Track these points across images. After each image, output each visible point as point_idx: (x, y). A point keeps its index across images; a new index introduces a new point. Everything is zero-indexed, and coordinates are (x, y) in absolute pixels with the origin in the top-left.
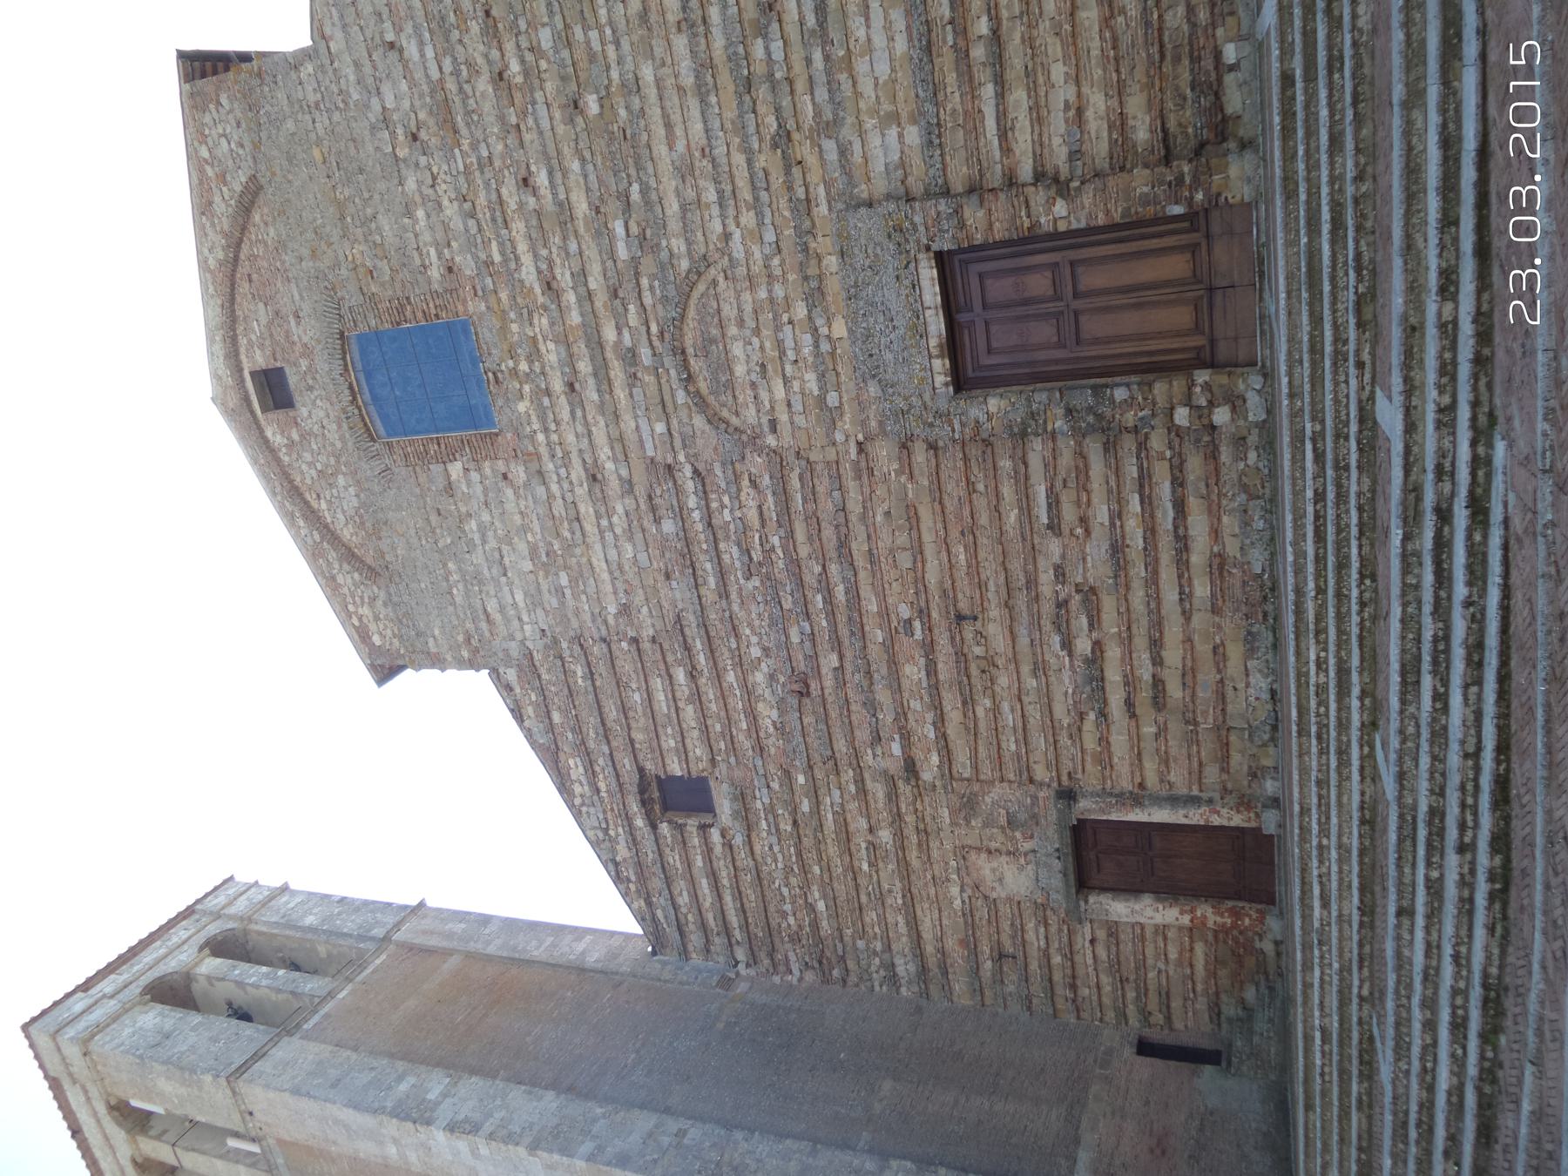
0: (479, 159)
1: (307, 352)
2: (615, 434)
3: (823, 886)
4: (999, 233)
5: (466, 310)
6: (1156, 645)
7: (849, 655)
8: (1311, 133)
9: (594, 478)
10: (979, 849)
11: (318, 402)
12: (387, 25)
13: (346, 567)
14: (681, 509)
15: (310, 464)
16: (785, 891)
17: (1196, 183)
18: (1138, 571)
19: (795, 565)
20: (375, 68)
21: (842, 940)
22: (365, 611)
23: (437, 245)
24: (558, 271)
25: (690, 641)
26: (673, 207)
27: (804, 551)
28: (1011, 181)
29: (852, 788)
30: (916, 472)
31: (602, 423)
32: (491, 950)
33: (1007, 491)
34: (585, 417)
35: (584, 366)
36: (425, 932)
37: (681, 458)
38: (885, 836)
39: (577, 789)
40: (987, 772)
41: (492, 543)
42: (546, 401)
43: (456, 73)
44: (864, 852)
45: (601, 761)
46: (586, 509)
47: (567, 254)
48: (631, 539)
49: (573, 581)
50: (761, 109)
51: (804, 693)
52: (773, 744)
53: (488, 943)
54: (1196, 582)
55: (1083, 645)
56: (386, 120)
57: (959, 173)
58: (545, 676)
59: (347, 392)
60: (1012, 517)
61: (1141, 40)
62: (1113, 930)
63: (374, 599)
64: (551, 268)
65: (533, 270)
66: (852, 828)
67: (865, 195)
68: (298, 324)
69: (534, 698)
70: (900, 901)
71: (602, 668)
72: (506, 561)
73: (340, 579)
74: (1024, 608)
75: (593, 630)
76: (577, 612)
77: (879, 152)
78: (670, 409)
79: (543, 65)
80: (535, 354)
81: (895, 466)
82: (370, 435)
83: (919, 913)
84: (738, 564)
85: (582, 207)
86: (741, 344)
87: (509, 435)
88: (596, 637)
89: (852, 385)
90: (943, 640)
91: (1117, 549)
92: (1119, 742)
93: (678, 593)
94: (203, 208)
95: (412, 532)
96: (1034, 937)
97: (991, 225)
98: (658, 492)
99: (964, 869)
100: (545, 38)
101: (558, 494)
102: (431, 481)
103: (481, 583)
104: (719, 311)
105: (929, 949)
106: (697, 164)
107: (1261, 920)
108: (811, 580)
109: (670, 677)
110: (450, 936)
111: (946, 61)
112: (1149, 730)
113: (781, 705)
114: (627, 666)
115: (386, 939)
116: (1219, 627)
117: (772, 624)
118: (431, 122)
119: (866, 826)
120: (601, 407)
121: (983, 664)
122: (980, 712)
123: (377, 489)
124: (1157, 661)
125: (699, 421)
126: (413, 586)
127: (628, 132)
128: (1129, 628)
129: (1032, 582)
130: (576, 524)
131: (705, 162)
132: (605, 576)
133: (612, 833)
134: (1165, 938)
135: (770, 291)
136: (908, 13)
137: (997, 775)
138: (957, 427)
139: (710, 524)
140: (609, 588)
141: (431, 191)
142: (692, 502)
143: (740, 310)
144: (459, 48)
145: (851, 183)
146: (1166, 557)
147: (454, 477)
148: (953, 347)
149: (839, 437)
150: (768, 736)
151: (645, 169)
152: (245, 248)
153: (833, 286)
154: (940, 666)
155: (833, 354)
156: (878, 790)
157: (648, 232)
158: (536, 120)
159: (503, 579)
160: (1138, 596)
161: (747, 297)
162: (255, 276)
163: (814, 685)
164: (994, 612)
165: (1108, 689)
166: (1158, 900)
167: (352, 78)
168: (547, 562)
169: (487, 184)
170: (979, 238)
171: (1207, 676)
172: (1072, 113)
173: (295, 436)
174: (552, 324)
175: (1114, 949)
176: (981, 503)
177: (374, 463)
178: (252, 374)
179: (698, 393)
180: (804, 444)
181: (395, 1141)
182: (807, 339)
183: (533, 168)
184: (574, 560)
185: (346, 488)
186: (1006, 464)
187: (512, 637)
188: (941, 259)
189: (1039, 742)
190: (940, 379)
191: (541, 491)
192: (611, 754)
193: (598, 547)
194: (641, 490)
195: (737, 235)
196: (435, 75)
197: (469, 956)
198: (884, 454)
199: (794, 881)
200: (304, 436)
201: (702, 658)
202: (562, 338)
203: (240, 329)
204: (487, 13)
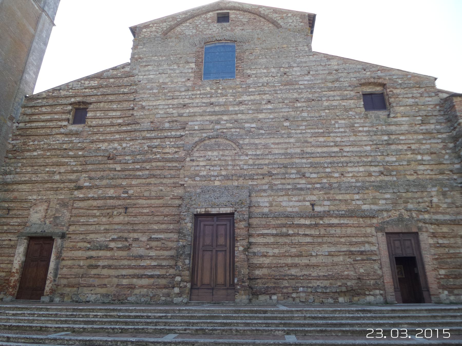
0: (277, 90)
1: (232, 30)
2: (197, 114)
3: (43, 155)
4: (237, 231)
5: (238, 78)
6: (109, 267)
7: (119, 173)
8: (251, 318)
9: (184, 106)
10: (48, 206)
11: (218, 30)
12: (314, 73)
13: (168, 26)
14: (172, 130)
16: (42, 143)
17: (242, 286)
18: (133, 263)
19: (150, 161)
20: (304, 67)
21: (22, 159)
22: (154, 29)
23: (256, 74)
24: (244, 106)
25: (131, 126)
26: (257, 141)
27: (154, 164)
28: (250, 236)
29: (75, 169)
30: (173, 200)
31: (200, 111)
32: (34, 44)
33: (164, 226)
34: (203, 106)
35: (217, 109)
36: (44, 24)
37: (187, 132)
38: (57, 177)
39: (87, 82)
40: (74, 211)
41: (169, 72)
42: (209, 96)
43: (300, 89)
44: (52, 170)
45: (95, 91)
47: (249, 110)
48: (165, 113)
49: (154, 94)
50: (279, 170)
51: (109, 158)
52: (94, 146)
53: (37, 43)
54: (127, 280)
55: (112, 245)
56: (291, 67)
57: (254, 221)
58: (125, 79)
59: (220, 39)
60: (155, 227)
61: (281, 273)
62: (14, 247)
63: (157, 32)
64: (245, 104)
65: (246, 99)
66: (61, 167)
67: (252, 195)
68: (241, 29)
69: (119, 74)
70: (33, 179)
71: (126, 97)
72: (163, 75)
73: (165, 24)
74: (127, 228)
75: (138, 97)
76: (144, 93)
77: (263, 200)
78: (202, 131)
79: (298, 113)
80: (222, 95)
82: (206, 43)
83: (28, 185)
84: (153, 144)
85: (261, 116)
86: (217, 155)
87: (200, 83)
88: (136, 97)
89: (201, 185)
91: (141, 257)
92: (79, 254)
93: (146, 124)
94: (275, 11)
95: (176, 49)
96: (14, 221)
97: (239, 229)
98: (178, 124)
99: (42, 201)
100: (305, 114)
101: (181, 94)
102: (190, 57)
103: (158, 66)
104: (227, 150)
105: (15, 187)
106: (267, 150)
107: (10, 295)
108: (145, 165)
109: (120, 118)
110: (41, 31)
111: (284, 221)
112: (82, 263)
114: (125, 105)
115: (43, 11)
116: (112, 286)
117: (133, 152)
118: (288, 79)
119: (61, 171)
120: (205, 112)
121: (111, 214)
124: (104, 267)
125: (197, 139)
126: (160, 45)
128: (116, 259)
129: (134, 231)
130: (171, 98)
131: (267, 152)
132: (154, 104)
133: (70, 91)
134: (8, 263)
135: (230, 165)
136: (297, 212)
137: (73, 215)
138: (184, 214)
139: (166, 137)
140: (151, 104)
141: (270, 75)
142: (173, 133)
143: (226, 156)
144: (306, 91)
145: (256, 191)
147: (191, 64)
148: (208, 215)
149: (186, 179)
150: (96, 145)
151: (268, 135)
152: (263, 20)
153: (229, 183)
154: (112, 201)
155: (210, 180)
156: (73, 177)
157: (251, 133)
158: (285, 108)
159: (158, 73)
160: (126, 262)
161: (230, 158)
162: (255, 20)
164: (126, 219)
165: (97, 251)
166: (23, 262)
167: (303, 60)
168: (161, 87)
169: (270, 91)
170: (236, 225)
171: (97, 282)
172: (265, 254)
173: (209, 21)
174: (230, 102)
175: (7, 246)
176: (161, 218)
177: (198, 42)
178: (228, 13)
179: (205, 140)
180: (186, 168)
182: (216, 174)
183: (272, 105)
184: (161, 95)
185: (192, 32)
186: (171, 227)
187: (139, 72)
188: (232, 214)
189: (82, 229)
190: (199, 210)
191: (183, 89)
192: (97, 95)
193: (164, 103)
194: (179, 119)
195: (247, 158)
196: (300, 83)
197: (33, 36)
198: (180, 191)
199: (46, 146)
201: (124, 128)
202: (226, 104)
203: (241, 12)
204: (313, 100)
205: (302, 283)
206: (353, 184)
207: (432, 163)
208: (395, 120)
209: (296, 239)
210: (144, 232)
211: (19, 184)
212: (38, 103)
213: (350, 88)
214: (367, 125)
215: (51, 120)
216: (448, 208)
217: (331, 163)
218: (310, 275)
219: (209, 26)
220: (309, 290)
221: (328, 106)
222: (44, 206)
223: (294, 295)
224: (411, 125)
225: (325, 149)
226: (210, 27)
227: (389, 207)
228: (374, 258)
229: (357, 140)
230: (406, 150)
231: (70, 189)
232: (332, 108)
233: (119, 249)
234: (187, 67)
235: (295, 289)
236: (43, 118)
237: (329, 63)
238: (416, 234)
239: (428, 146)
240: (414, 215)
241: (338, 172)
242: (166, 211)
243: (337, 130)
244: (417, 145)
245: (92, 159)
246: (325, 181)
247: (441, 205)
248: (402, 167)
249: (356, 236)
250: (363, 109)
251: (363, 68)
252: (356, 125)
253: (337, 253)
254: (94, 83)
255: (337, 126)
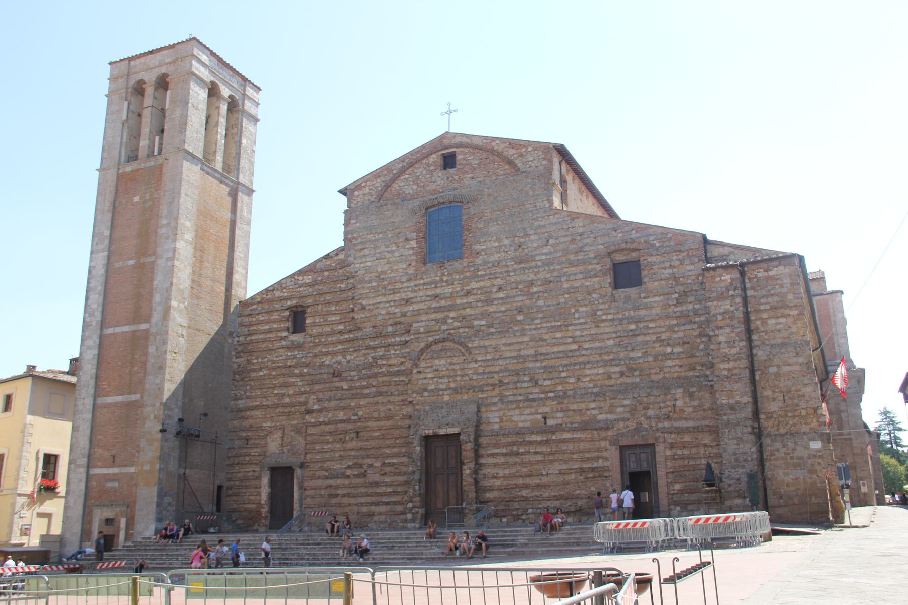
1: (460, 180)
4: (464, 453)
7: (347, 392)
10: (283, 434)
13: (384, 184)
15: (421, 172)
16: (266, 360)
18: (371, 490)
19: (376, 375)
22: (367, 190)
23: (486, 249)
24: (473, 297)
27: (380, 379)
29: (302, 390)
33: (396, 450)
35: (443, 303)
38: (287, 400)
39: (300, 278)
40: (309, 438)
42: (433, 286)
43: (536, 267)
44: (281, 392)
45: (311, 290)
46: (397, 297)
47: (477, 302)
49: (373, 288)
52: (317, 361)
55: (348, 472)
56: (528, 235)
58: (341, 271)
62: (259, 478)
63: (371, 194)
64: (474, 294)
66: (290, 388)
71: (344, 296)
72: (381, 260)
73: (379, 180)
76: (363, 288)
78: (428, 334)
79: (534, 301)
81: (405, 413)
85: (491, 309)
88: (355, 295)
90: (350, 426)
91: (377, 484)
92: (320, 482)
93: (368, 330)
94: (513, 144)
95: (393, 220)
96: (254, 451)
100: (541, 303)
103: (374, 248)
105: (248, 413)
107: (264, 525)
108: (371, 381)
110: (242, 211)
112: (323, 492)
113: (330, 366)
114: (344, 306)
117: (357, 365)
121: (343, 440)
122: (328, 437)
123: (409, 207)
124: (344, 495)
125: (422, 345)
127: (510, 330)
129: (368, 457)
130: (392, 292)
132: (375, 301)
136: (528, 427)
139: (390, 345)
140: (371, 302)
142: (398, 339)
144: (543, 269)
146: (374, 499)
147: (411, 242)
148: (436, 436)
149: (414, 395)
150: (320, 359)
152: (497, 159)
153: (459, 397)
155: (439, 395)
156: (302, 399)
157: (481, 333)
160: (363, 490)
162: (488, 161)
163: (337, 379)
164: (359, 444)
166: (269, 494)
168: (379, 278)
169: (501, 273)
170: (463, 447)
173: (432, 168)
174: (457, 292)
176: (393, 441)
177: (418, 208)
179: (431, 346)
181: (169, 224)
182: (444, 387)
186: (403, 450)
187: (355, 259)
188: (459, 434)
189: (318, 457)
190: (427, 432)
191: (404, 279)
193: (385, 300)
194: (402, 319)
195: (476, 365)
196: (537, 258)
198: (409, 410)
199: (270, 363)
200: (431, 173)
201: (346, 336)
203: (471, 150)
204: (551, 282)
205: (532, 504)
206: (590, 390)
207: (683, 356)
208: (646, 301)
209: (526, 458)
210: (377, 458)
211: (252, 410)
212: (254, 309)
213: (595, 261)
214: (611, 311)
215: (270, 331)
216: (694, 412)
217: (566, 365)
218: (541, 495)
219: (432, 176)
220: (538, 511)
221: (568, 289)
222: (280, 434)
223: (524, 517)
224: (667, 306)
225: (562, 348)
226: (433, 178)
227: (627, 415)
228: (606, 475)
229: (599, 332)
230: (654, 342)
231: (301, 413)
232: (573, 291)
233: (356, 476)
234: (407, 246)
235: (525, 511)
236: (261, 328)
237: (573, 225)
238: (653, 445)
239: (681, 334)
240: (654, 424)
241: (574, 376)
242: (396, 433)
243: (577, 322)
244: (668, 334)
245: (318, 377)
246: (560, 388)
247: (685, 409)
248: (647, 364)
249: (589, 451)
250: (610, 290)
251: (614, 228)
252: (599, 313)
253: (567, 471)
254: (308, 279)
255: (576, 315)
